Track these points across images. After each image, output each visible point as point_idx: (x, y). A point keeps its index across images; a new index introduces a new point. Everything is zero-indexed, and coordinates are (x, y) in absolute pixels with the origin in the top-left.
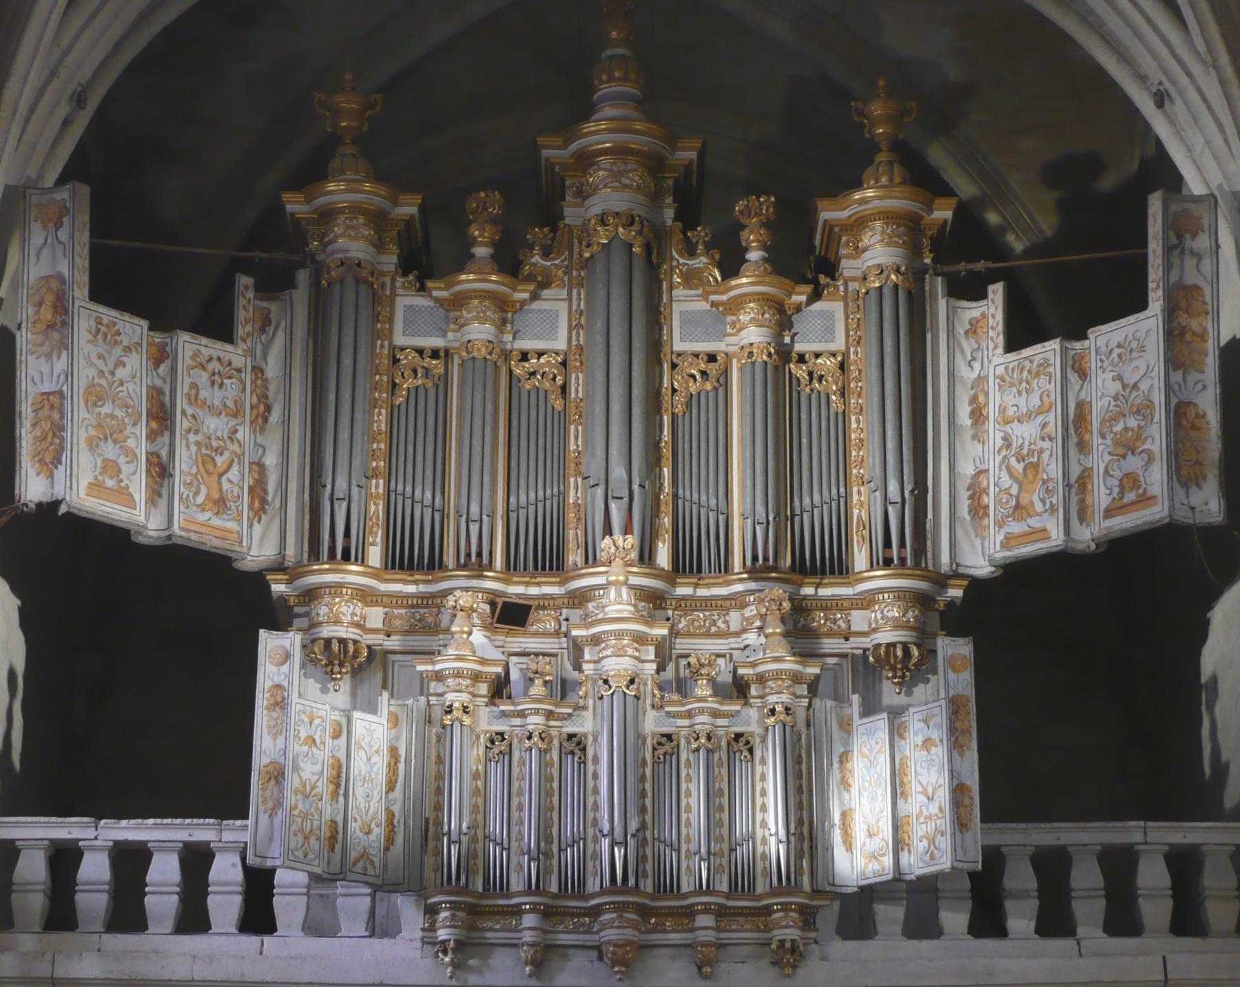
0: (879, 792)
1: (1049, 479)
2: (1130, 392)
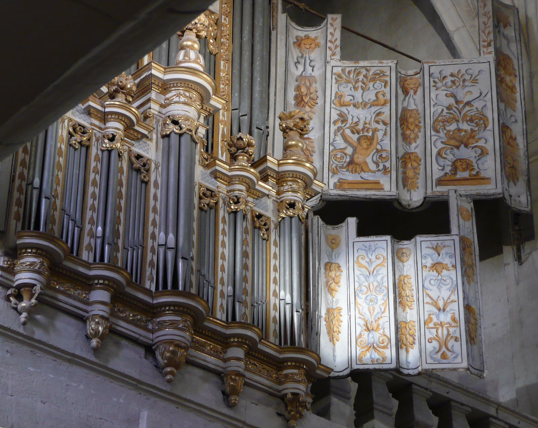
0: (380, 297)
1: (382, 150)
2: (464, 107)
